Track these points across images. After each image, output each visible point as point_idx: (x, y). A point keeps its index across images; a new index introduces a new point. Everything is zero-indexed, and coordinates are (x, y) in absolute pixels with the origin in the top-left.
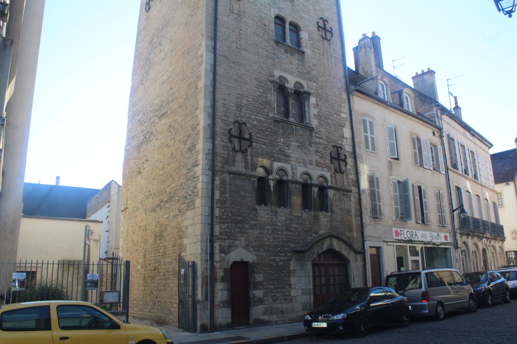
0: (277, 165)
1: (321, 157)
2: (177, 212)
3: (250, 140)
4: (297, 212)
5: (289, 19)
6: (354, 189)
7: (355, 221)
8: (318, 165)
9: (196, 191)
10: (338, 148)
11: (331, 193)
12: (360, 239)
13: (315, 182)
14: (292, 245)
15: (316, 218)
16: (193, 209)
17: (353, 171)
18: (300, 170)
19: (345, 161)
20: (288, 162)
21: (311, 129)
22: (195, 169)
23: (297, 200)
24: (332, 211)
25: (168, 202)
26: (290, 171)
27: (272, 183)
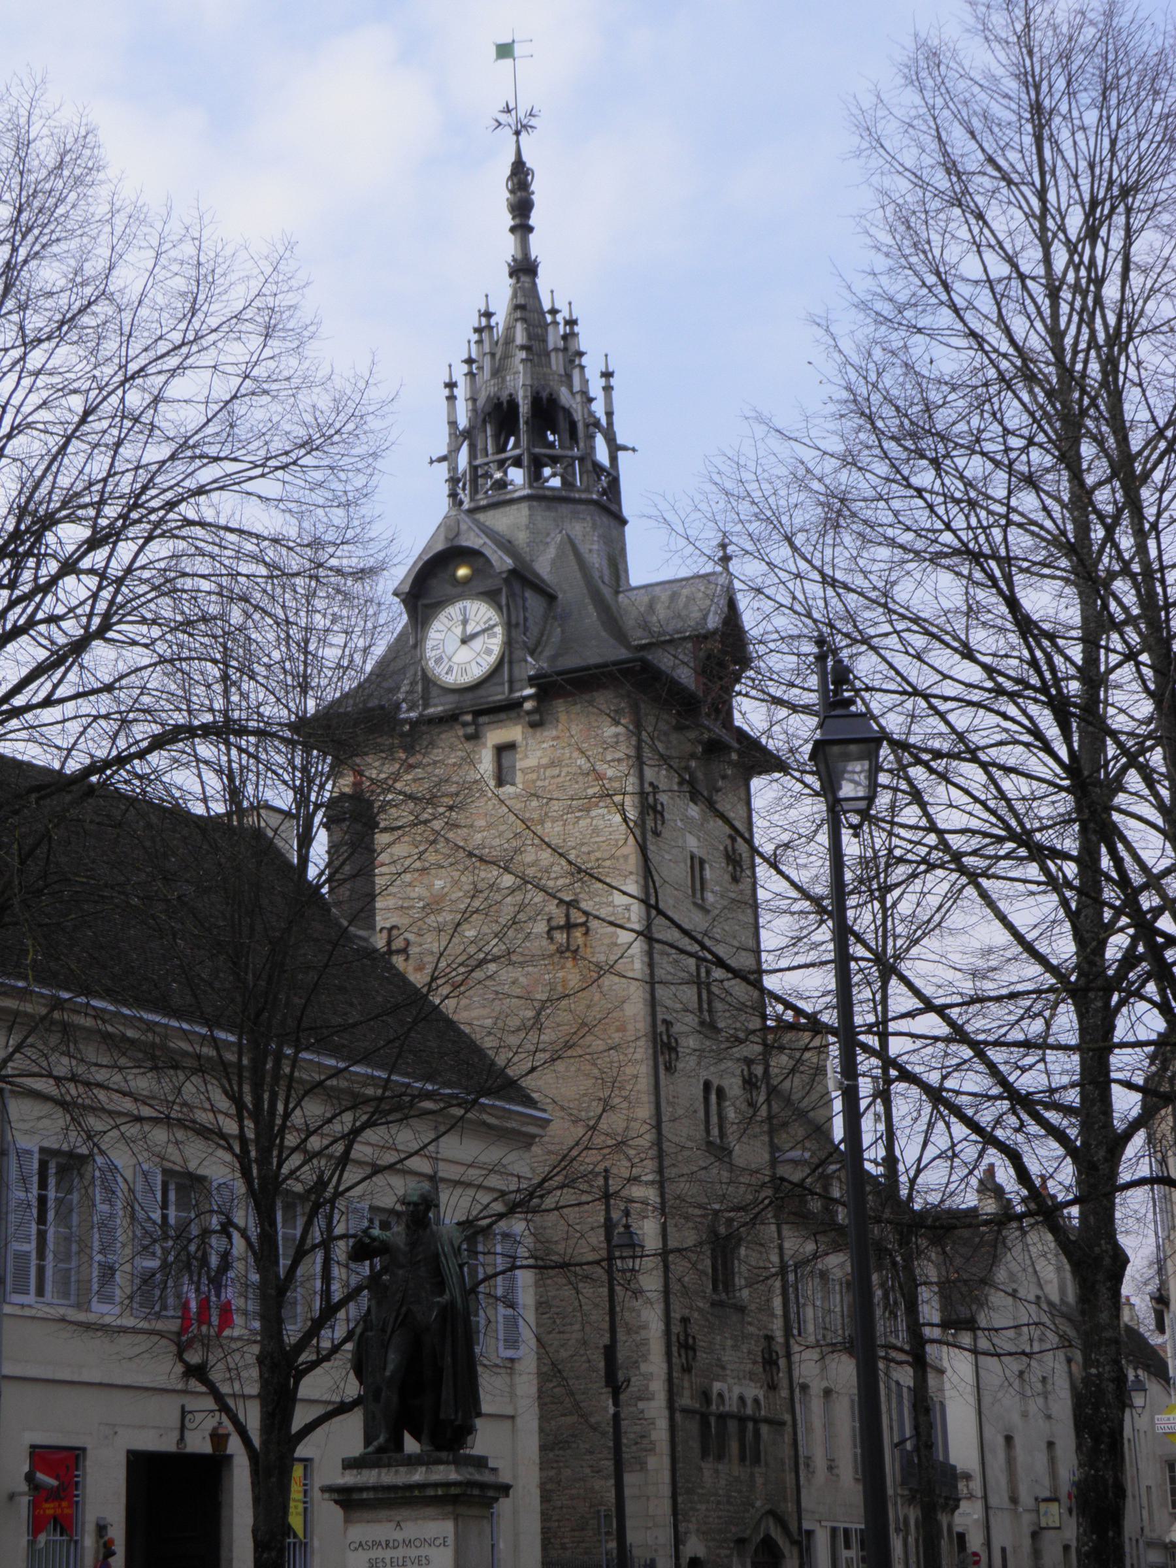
0: (717, 1386)
1: (755, 1363)
2: (588, 1471)
3: (694, 1350)
4: (736, 1470)
5: (716, 1083)
6: (787, 1417)
7: (789, 1478)
8: (752, 1376)
9: (645, 1441)
10: (769, 1338)
11: (764, 1429)
12: (795, 1516)
13: (749, 1411)
14: (734, 1529)
15: (752, 1475)
16: (642, 1469)
17: (784, 1383)
18: (736, 1391)
19: (776, 1364)
20: (724, 1381)
21: (741, 1309)
22: (641, 1405)
23: (734, 1446)
24: (767, 1465)
25: (552, 1450)
26: (727, 1395)
27: (713, 1420)
